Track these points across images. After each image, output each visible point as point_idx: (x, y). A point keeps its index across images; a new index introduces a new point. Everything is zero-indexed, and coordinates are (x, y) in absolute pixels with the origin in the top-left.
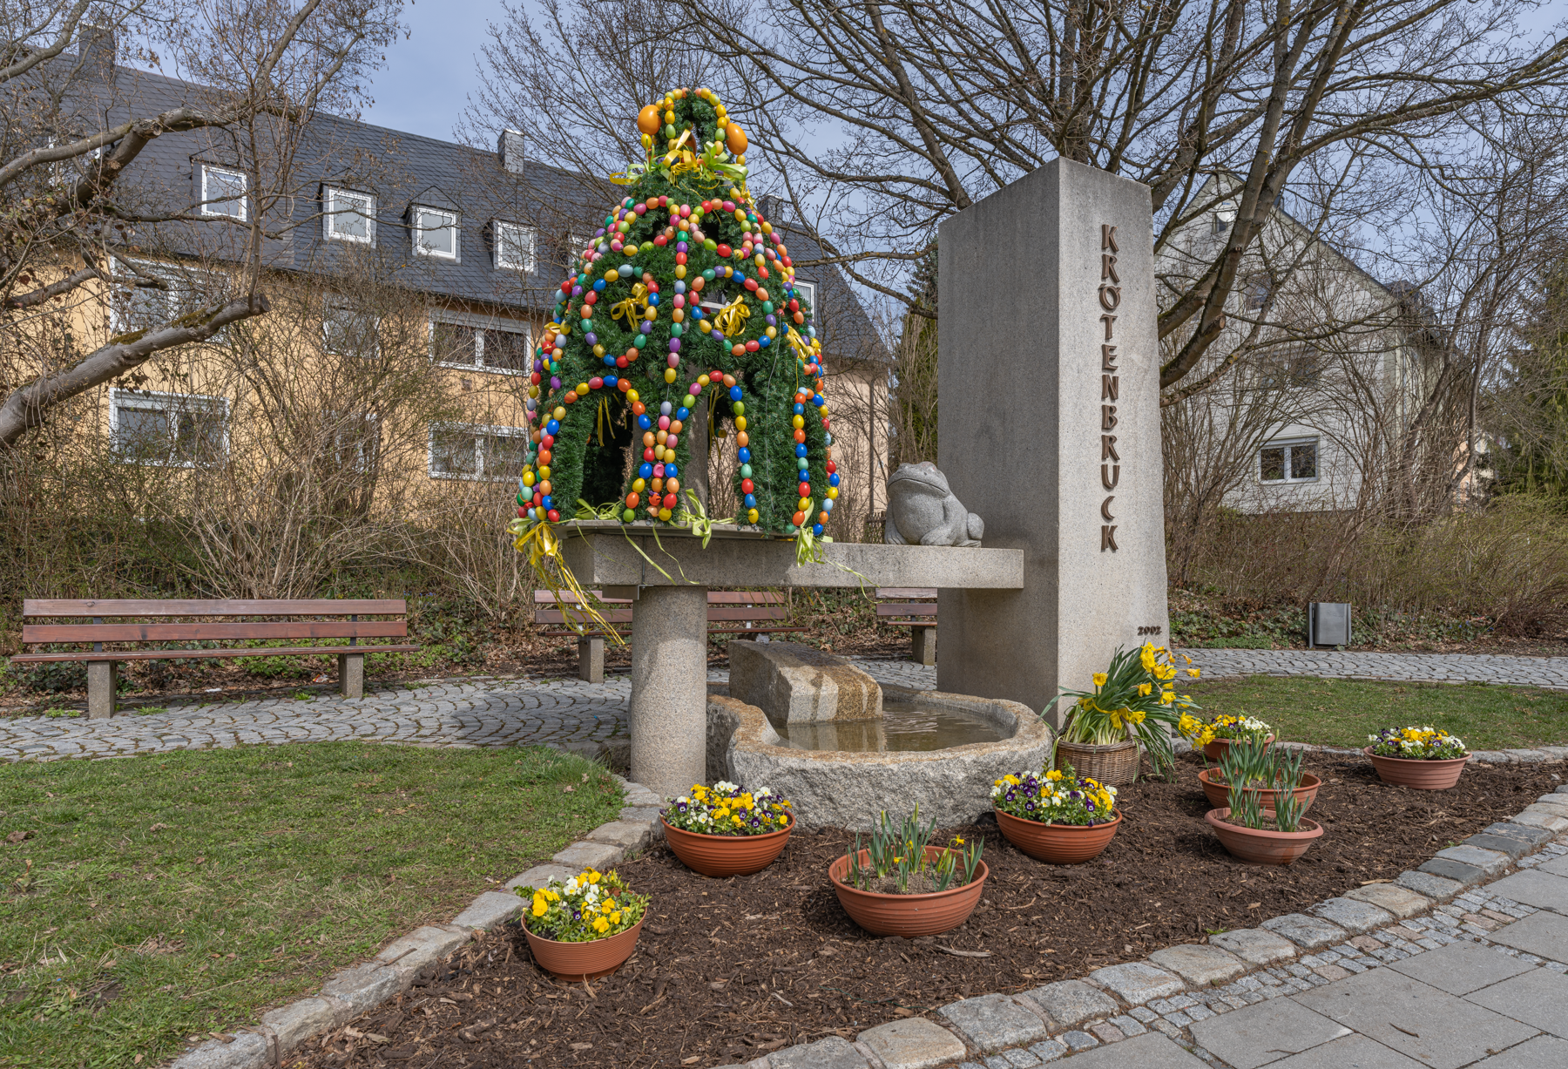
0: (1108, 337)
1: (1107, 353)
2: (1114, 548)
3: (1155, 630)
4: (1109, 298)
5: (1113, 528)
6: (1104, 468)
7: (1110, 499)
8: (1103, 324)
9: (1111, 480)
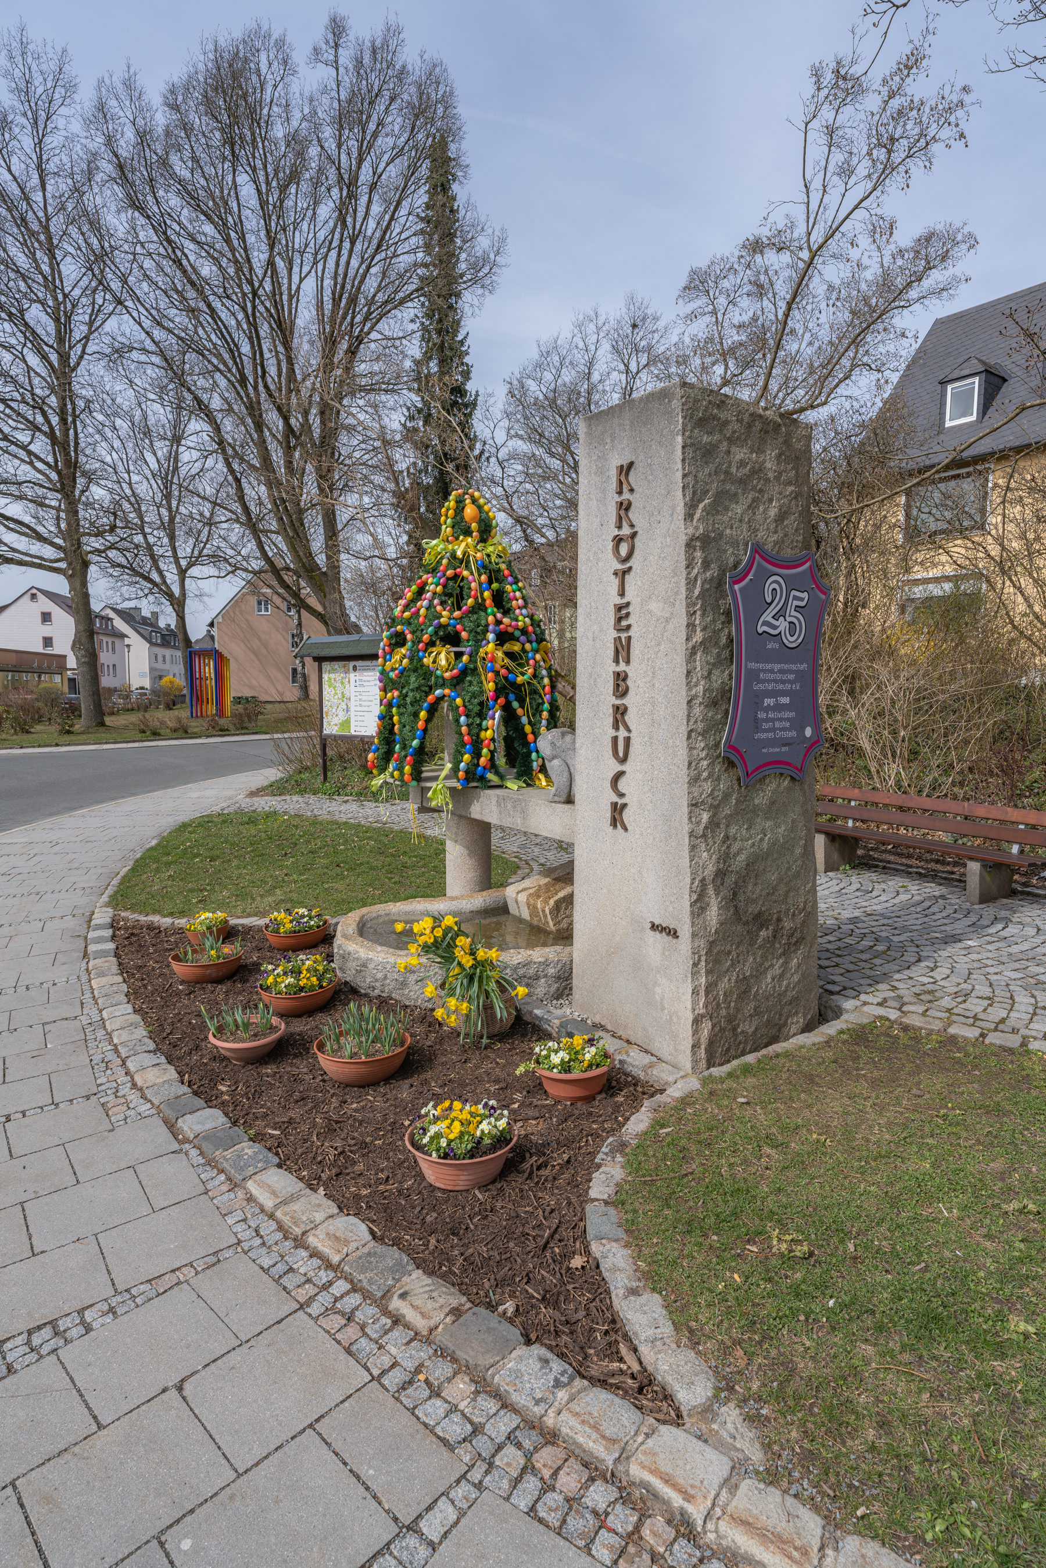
0: (622, 594)
1: (622, 612)
2: (626, 829)
3: (673, 933)
4: (625, 545)
5: (625, 806)
6: (615, 739)
7: (620, 775)
8: (615, 582)
9: (621, 754)
